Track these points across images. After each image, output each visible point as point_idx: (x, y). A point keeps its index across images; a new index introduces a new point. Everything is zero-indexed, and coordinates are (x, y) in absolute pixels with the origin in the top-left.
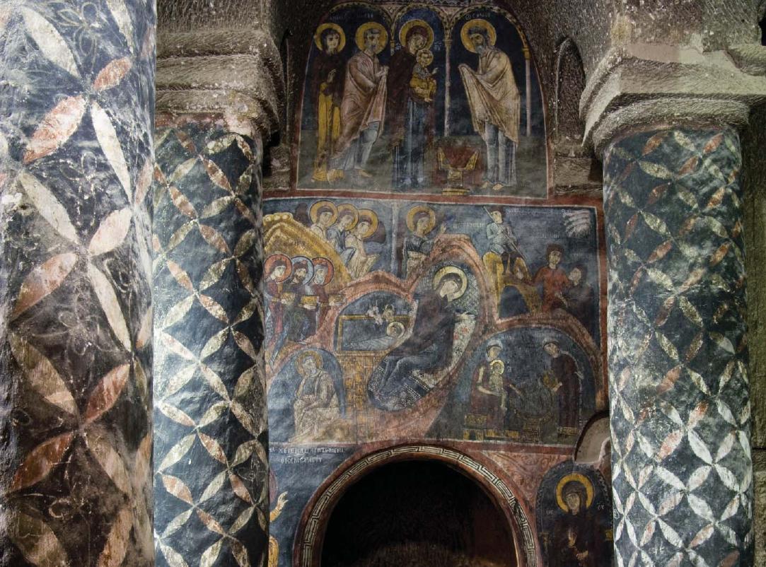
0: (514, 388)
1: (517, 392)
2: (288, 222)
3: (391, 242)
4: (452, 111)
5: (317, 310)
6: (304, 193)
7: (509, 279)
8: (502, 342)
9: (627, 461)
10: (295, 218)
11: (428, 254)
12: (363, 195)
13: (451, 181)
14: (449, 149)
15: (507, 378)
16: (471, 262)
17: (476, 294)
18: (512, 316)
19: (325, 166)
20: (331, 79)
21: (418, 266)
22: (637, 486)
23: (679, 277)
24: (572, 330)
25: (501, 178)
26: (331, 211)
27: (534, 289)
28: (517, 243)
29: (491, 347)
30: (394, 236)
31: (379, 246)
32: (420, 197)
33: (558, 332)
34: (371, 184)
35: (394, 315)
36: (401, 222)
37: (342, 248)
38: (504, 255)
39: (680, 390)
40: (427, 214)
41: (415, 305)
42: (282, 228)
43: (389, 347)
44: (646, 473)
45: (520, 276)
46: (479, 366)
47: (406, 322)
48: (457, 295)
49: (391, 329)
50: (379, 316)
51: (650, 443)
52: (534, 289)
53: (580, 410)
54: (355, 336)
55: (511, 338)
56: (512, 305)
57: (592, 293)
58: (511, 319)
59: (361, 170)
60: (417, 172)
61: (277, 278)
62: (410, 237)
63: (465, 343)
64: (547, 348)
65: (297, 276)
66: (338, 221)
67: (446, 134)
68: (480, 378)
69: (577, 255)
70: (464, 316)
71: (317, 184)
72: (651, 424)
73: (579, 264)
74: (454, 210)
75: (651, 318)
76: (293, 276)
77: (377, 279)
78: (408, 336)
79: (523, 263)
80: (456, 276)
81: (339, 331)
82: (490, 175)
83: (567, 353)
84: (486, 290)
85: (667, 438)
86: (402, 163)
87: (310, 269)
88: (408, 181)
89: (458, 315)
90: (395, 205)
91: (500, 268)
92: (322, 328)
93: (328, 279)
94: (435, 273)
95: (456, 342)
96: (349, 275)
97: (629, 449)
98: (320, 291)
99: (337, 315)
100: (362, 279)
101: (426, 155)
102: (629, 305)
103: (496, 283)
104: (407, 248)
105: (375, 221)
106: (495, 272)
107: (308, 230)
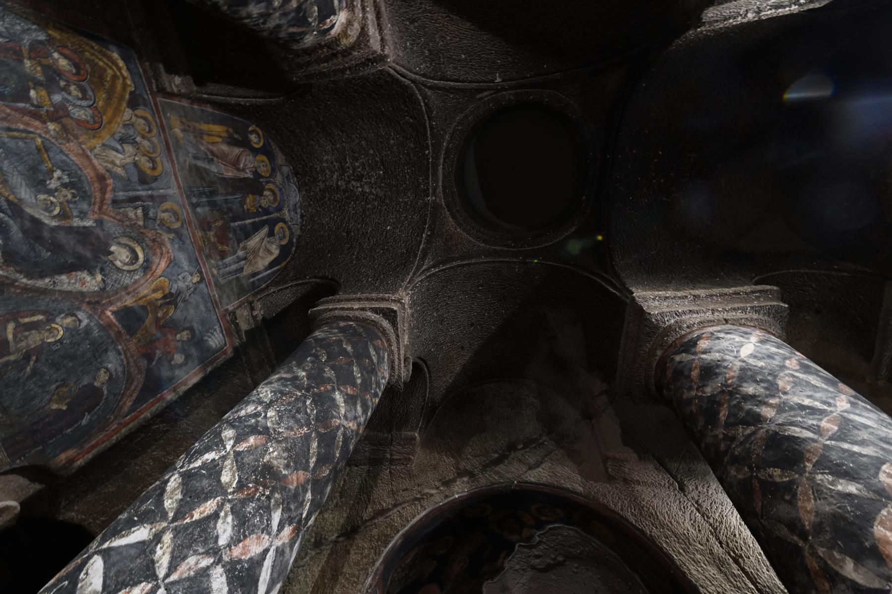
0: (32, 363)
1: (28, 369)
2: (125, 85)
3: (143, 190)
4: (245, 226)
5: (33, 105)
6: (156, 104)
7: (153, 306)
8: (88, 325)
9: (177, 532)
10: (131, 93)
11: (145, 227)
12: (172, 161)
13: (206, 234)
14: (225, 228)
15: (41, 349)
16: (154, 268)
17: (127, 281)
18: (120, 323)
19: (182, 127)
20: (236, 136)
21: (130, 219)
22: (167, 575)
23: (349, 415)
24: (131, 384)
25: (221, 271)
26: (150, 131)
27: (154, 330)
28: (184, 301)
29: (76, 317)
30: (150, 192)
31: (135, 178)
32: (186, 212)
33: (124, 372)
34: (182, 169)
35: (68, 201)
36: (163, 198)
37: (120, 140)
38: (171, 294)
39: (296, 496)
40: (178, 220)
41: (89, 223)
42: (115, 77)
43: (20, 200)
44: (197, 563)
45: (160, 315)
46: (43, 313)
47: (63, 215)
48: (118, 263)
49: (45, 199)
50: (58, 183)
51: (234, 527)
52: (154, 330)
53: (41, 447)
54: (17, 154)
55: (96, 333)
56: (130, 318)
57: (171, 379)
58: (117, 323)
59: (190, 160)
60: (203, 206)
61: (57, 60)
62: (154, 208)
63: (66, 287)
64: (102, 371)
65: (68, 85)
66: (143, 137)
67: (232, 224)
68: (27, 320)
69: (194, 351)
70: (99, 277)
71: (168, 119)
72: (250, 507)
73: (188, 357)
74: (188, 242)
75: (317, 419)
76: (68, 81)
77: (101, 179)
78: (46, 221)
79: (172, 312)
80: (136, 257)
81: (15, 134)
82: (220, 263)
83: (105, 393)
84: (135, 289)
85: (254, 536)
86: (204, 193)
87: (84, 103)
88: (194, 200)
89: (98, 271)
90: (173, 191)
91: (159, 295)
92: (8, 111)
93: (79, 122)
94: (130, 237)
95: (64, 277)
96: (95, 148)
97: (196, 516)
98: (61, 113)
99: (38, 131)
100: (95, 162)
101: (215, 212)
102: (306, 397)
103: (145, 296)
104: (143, 206)
105: (156, 173)
106: (155, 291)
107: (124, 105)
